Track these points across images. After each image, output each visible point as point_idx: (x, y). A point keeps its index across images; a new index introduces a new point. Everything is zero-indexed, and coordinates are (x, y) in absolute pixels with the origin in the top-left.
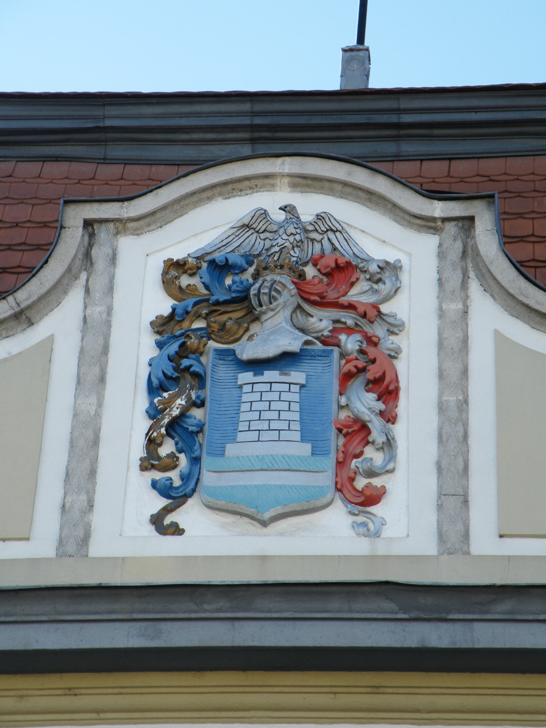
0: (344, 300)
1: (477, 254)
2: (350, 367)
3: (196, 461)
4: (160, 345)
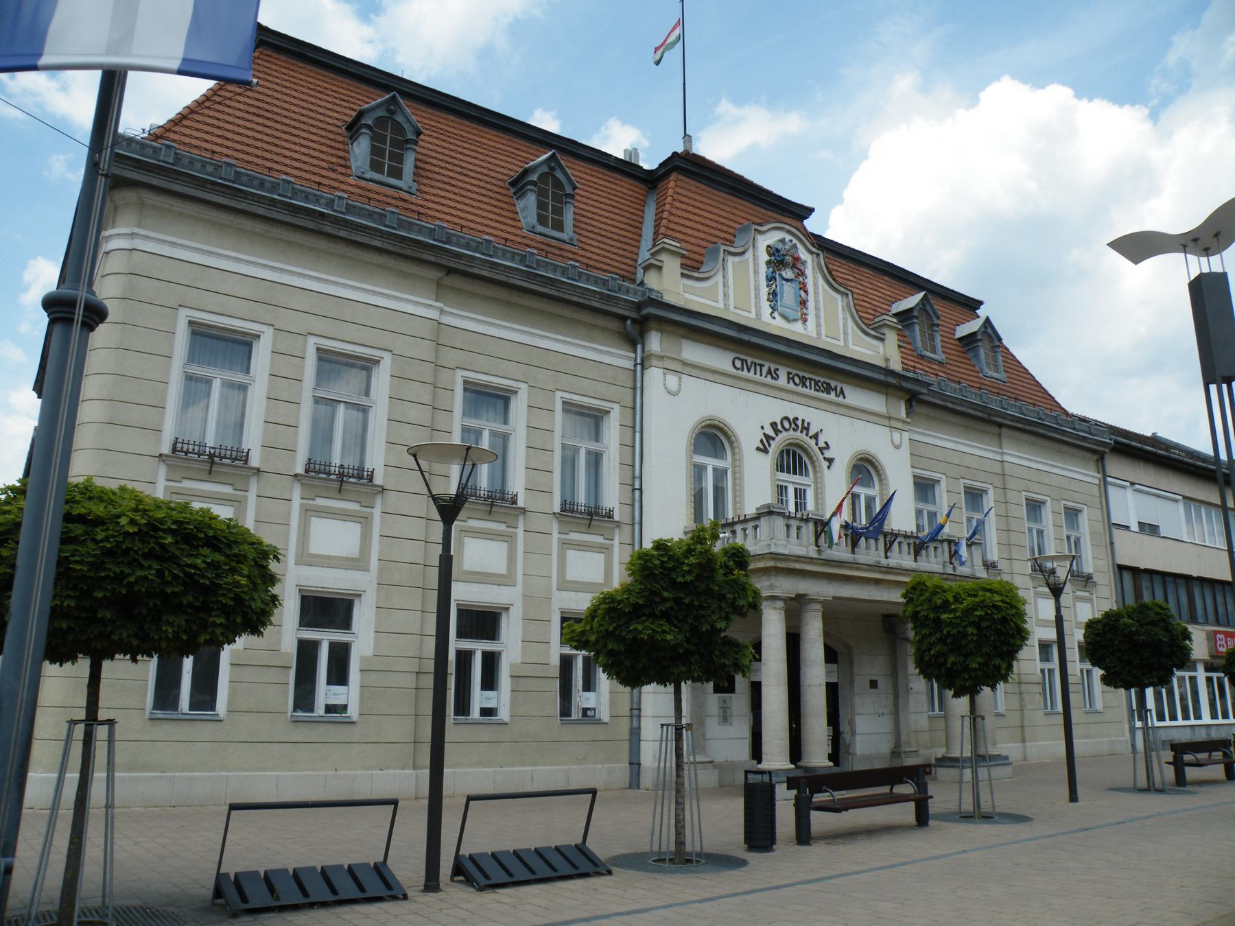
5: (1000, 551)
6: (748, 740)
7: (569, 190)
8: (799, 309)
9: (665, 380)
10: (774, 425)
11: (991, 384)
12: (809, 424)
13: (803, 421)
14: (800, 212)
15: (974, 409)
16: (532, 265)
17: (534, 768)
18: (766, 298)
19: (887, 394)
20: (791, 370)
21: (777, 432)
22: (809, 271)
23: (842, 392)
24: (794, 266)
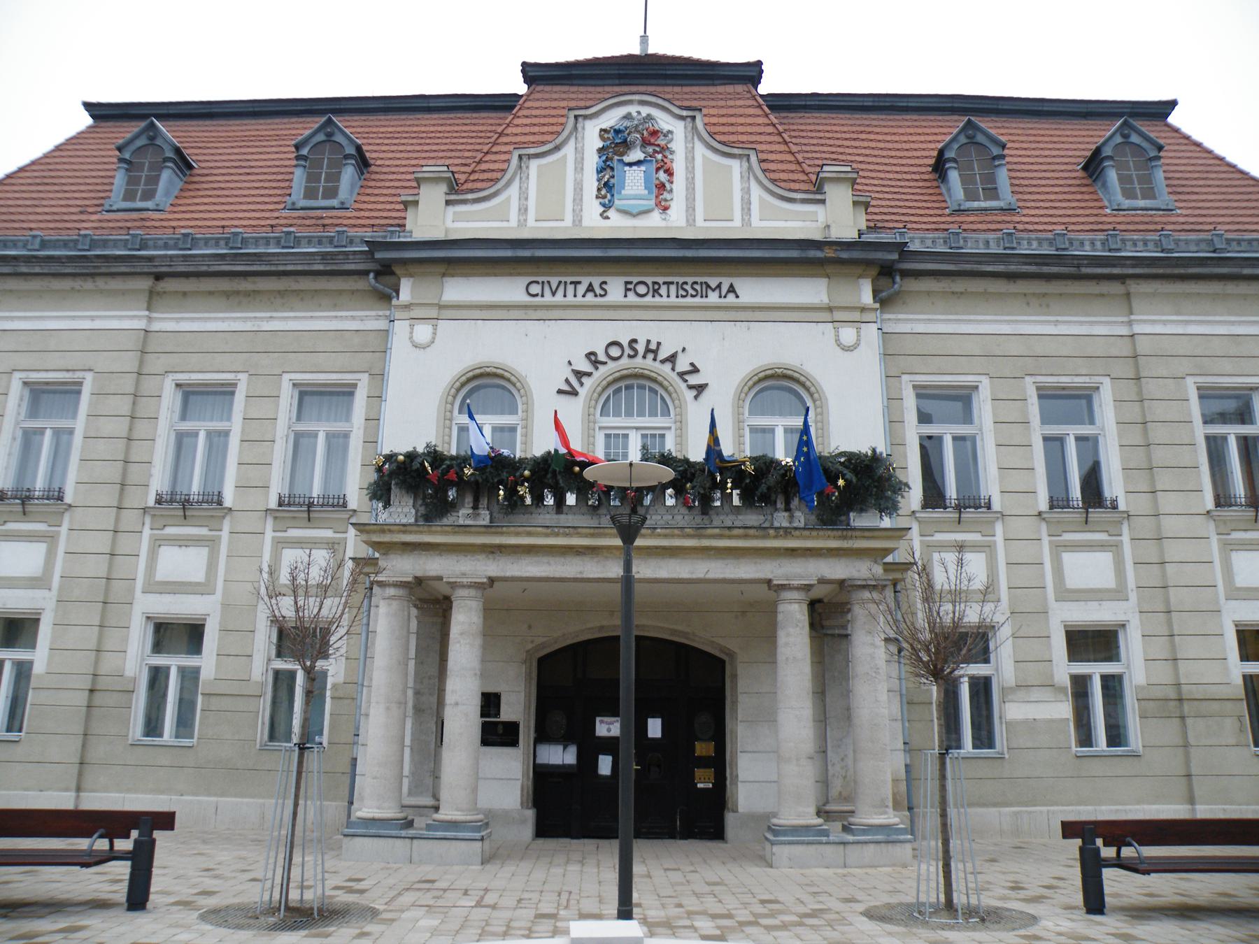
0: (656, 143)
1: (696, 128)
2: (659, 165)
3: (613, 196)
4: (600, 157)
5: (1127, 479)
6: (519, 784)
7: (996, 151)
8: (653, 196)
9: (411, 333)
10: (591, 356)
11: (1128, 220)
12: (659, 344)
13: (649, 342)
14: (751, 73)
15: (1037, 264)
16: (1012, 245)
17: (220, 799)
18: (595, 192)
19: (828, 276)
22: (678, 145)
23: (732, 289)
24: (645, 143)
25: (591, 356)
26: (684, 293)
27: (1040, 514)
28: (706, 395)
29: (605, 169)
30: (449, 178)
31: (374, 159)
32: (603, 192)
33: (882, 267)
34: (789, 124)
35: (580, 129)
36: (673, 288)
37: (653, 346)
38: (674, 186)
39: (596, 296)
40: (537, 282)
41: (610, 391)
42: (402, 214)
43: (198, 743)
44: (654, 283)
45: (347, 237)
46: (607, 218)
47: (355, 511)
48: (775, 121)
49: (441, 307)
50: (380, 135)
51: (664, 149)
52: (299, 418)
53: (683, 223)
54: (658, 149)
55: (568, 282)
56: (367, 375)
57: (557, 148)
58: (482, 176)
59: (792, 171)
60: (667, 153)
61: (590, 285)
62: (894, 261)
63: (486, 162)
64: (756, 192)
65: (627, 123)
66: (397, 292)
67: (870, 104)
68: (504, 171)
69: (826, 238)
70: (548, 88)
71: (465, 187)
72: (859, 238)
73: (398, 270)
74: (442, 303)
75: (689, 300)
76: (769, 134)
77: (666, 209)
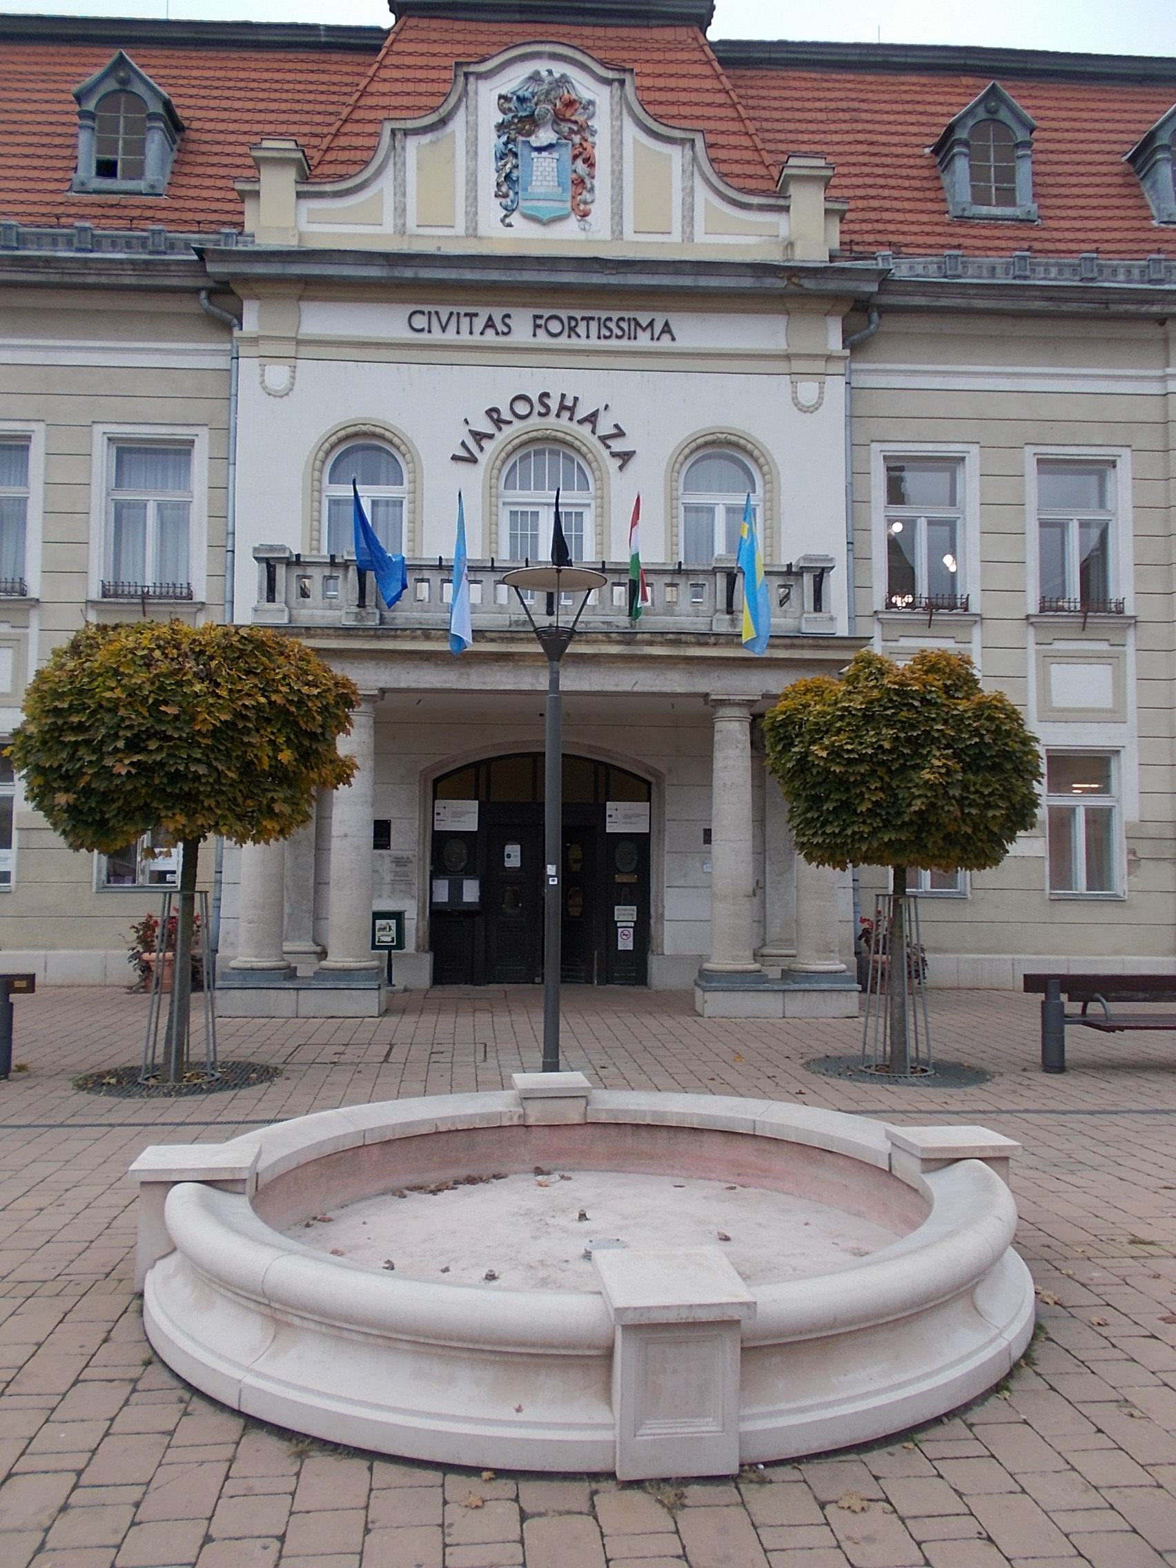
0: (573, 118)
1: (626, 99)
2: (576, 152)
5: (1138, 578)
8: (568, 196)
9: (263, 375)
10: (492, 413)
12: (576, 399)
13: (563, 396)
20: (539, 312)
21: (499, 422)
22: (601, 122)
23: (667, 329)
24: (559, 118)
25: (492, 413)
26: (608, 334)
27: (1028, 617)
28: (633, 464)
29: (506, 155)
30: (299, 160)
31: (187, 119)
32: (504, 189)
33: (857, 301)
34: (747, 87)
35: (471, 94)
36: (594, 325)
37: (569, 402)
38: (596, 182)
39: (497, 333)
40: (422, 313)
41: (516, 457)
42: (238, 207)
43: (17, 887)
44: (570, 318)
45: (166, 239)
46: (510, 225)
47: (203, 603)
48: (728, 86)
49: (299, 342)
50: (194, 82)
51: (583, 129)
52: (119, 484)
53: (606, 234)
54: (575, 128)
55: (462, 313)
56: (206, 429)
57: (443, 122)
58: (345, 156)
59: (748, 162)
60: (587, 135)
61: (490, 318)
62: (872, 294)
63: (346, 134)
64: (702, 194)
65: (534, 87)
66: (240, 318)
67: (855, 58)
68: (374, 149)
69: (788, 260)
70: (424, 23)
71: (318, 171)
72: (831, 261)
73: (239, 290)
74: (300, 337)
75: (613, 343)
76: (720, 105)
77: (585, 215)
